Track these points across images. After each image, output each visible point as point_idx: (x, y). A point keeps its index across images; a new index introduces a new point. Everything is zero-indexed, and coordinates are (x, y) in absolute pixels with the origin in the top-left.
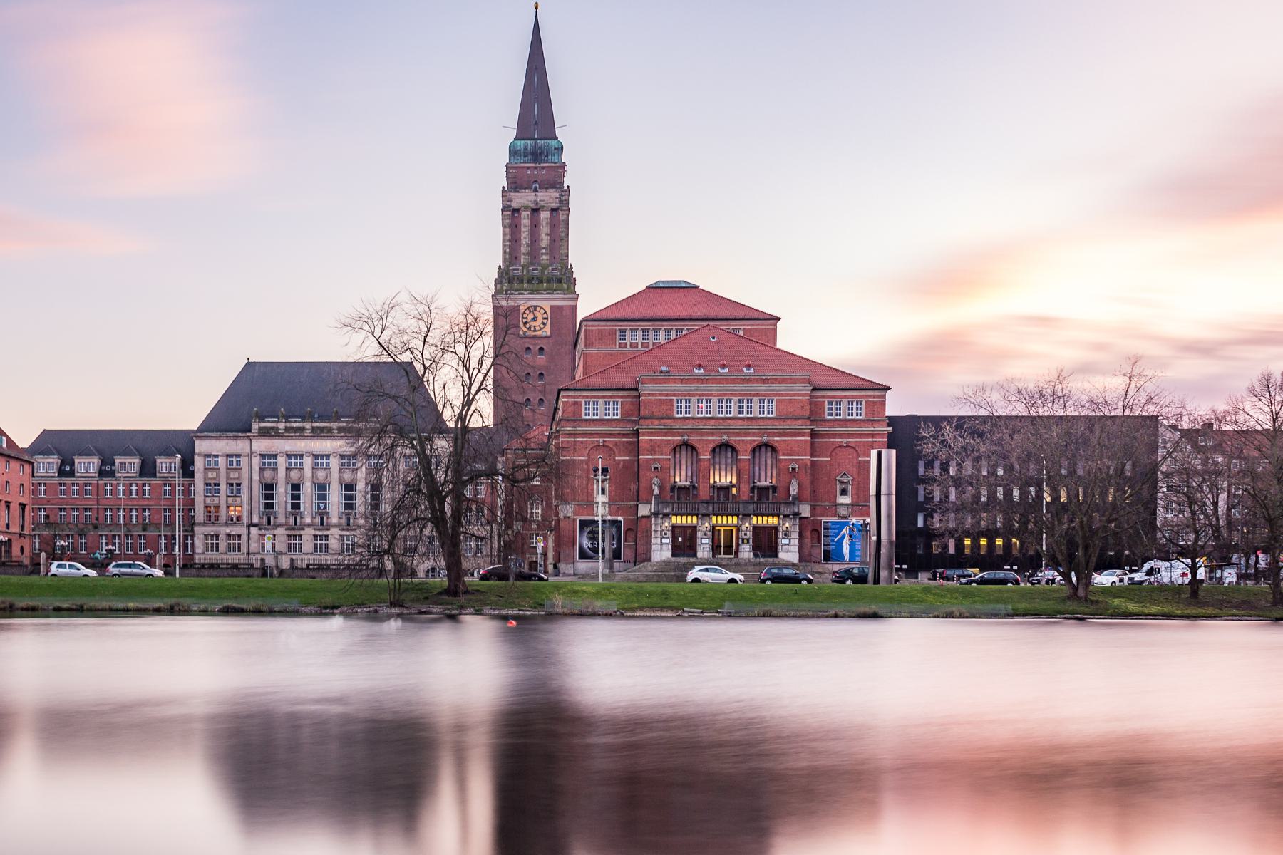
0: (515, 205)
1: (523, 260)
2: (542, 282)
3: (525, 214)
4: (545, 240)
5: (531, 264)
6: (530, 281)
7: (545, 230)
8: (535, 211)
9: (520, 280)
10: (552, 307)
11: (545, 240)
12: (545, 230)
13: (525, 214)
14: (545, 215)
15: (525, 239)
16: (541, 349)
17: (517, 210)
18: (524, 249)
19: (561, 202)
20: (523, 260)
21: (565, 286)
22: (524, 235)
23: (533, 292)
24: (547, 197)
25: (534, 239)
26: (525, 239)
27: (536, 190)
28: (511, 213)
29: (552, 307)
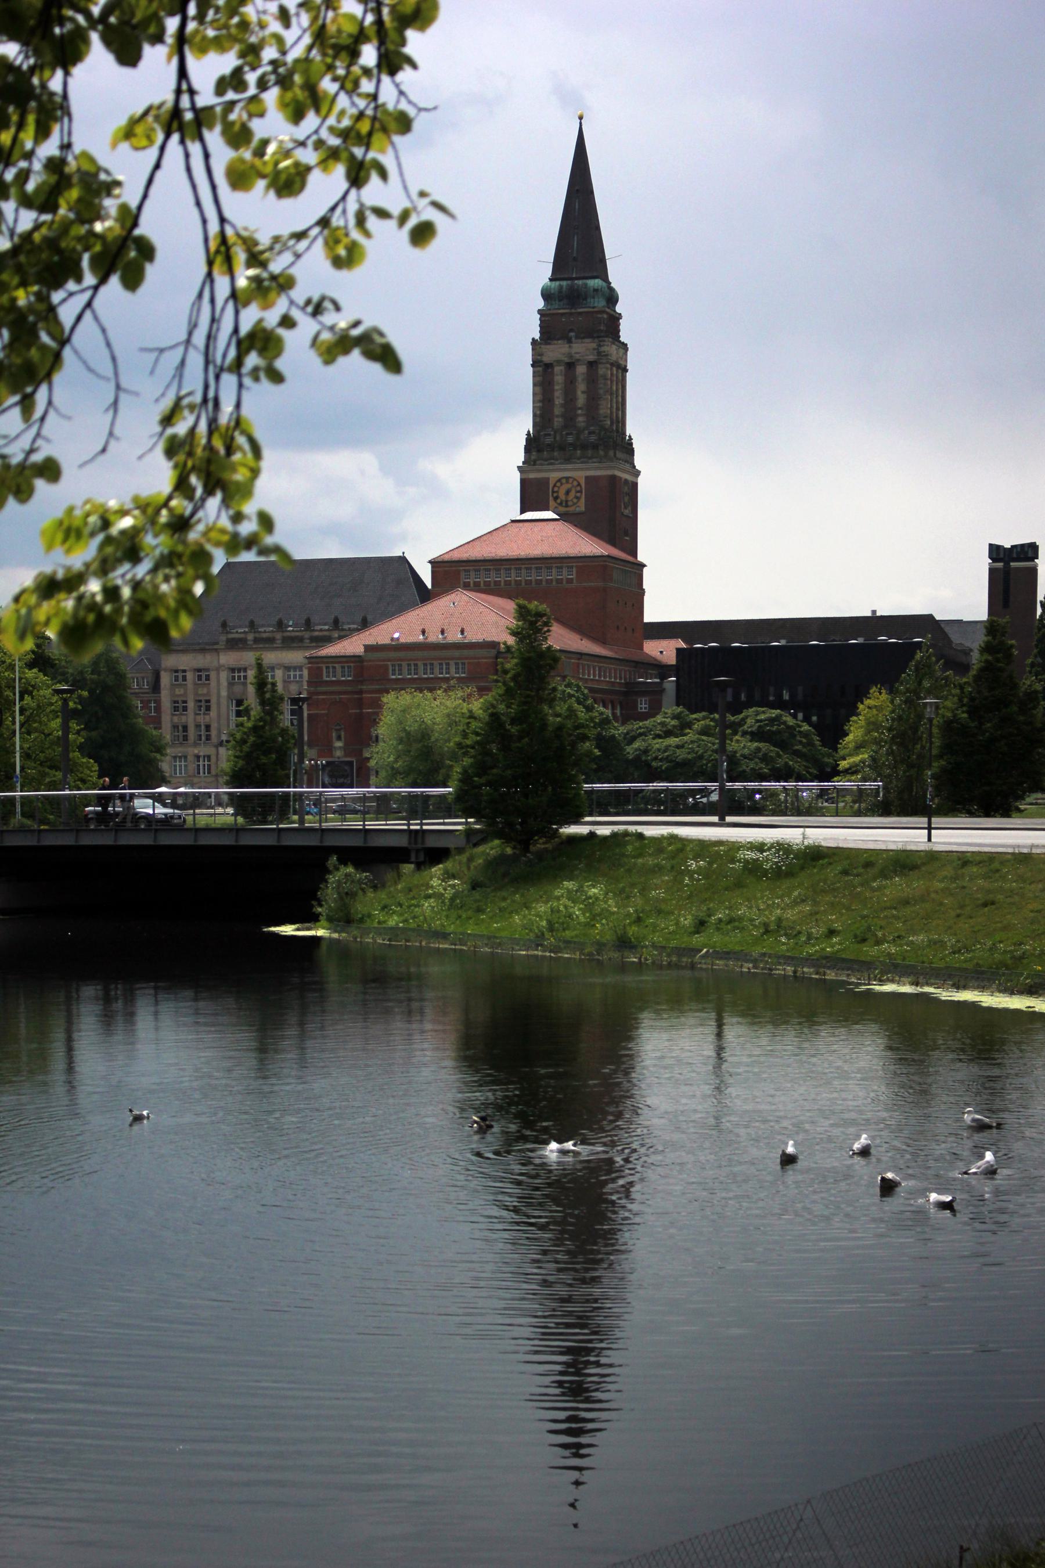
0: (546, 359)
1: (558, 422)
2: (575, 449)
4: (581, 399)
5: (566, 427)
6: (562, 448)
7: (581, 387)
8: (570, 366)
9: (551, 447)
10: (587, 478)
11: (581, 399)
12: (581, 387)
13: (558, 369)
14: (581, 370)
15: (559, 400)
17: (548, 366)
18: (557, 411)
19: (599, 353)
20: (558, 422)
21: (602, 453)
22: (557, 394)
23: (568, 460)
26: (559, 400)
27: (570, 341)
28: (542, 368)
29: (587, 478)
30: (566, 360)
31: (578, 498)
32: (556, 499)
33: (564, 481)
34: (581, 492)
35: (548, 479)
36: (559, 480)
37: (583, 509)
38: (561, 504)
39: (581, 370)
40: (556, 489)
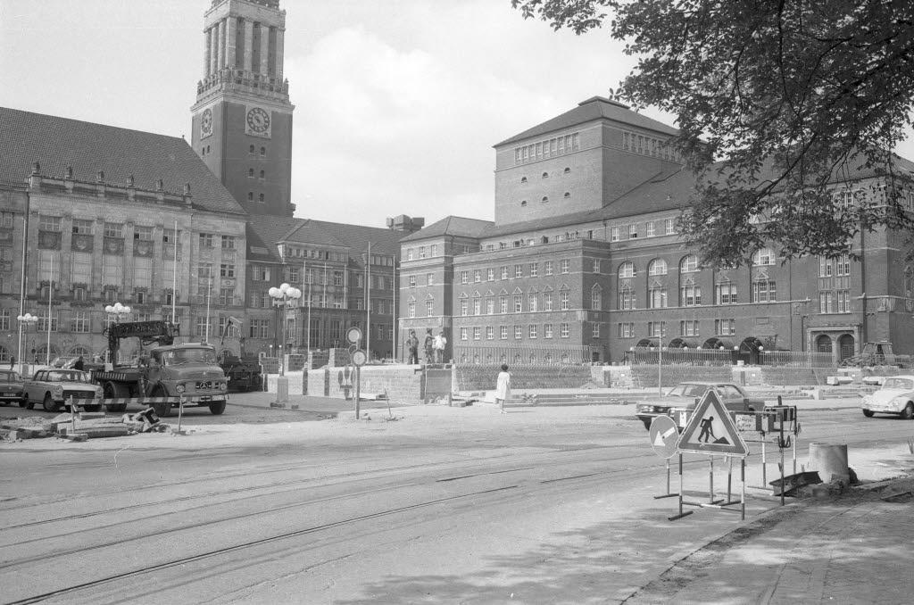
0: (243, 14)
3: (249, 27)
10: (273, 112)
13: (249, 27)
14: (264, 30)
16: (263, 149)
24: (264, 14)
25: (256, 52)
29: (273, 112)
30: (255, 18)
31: (266, 127)
32: (250, 123)
33: (256, 111)
34: (268, 122)
35: (243, 107)
36: (253, 110)
37: (270, 136)
38: (254, 129)
39: (264, 30)
40: (250, 116)
